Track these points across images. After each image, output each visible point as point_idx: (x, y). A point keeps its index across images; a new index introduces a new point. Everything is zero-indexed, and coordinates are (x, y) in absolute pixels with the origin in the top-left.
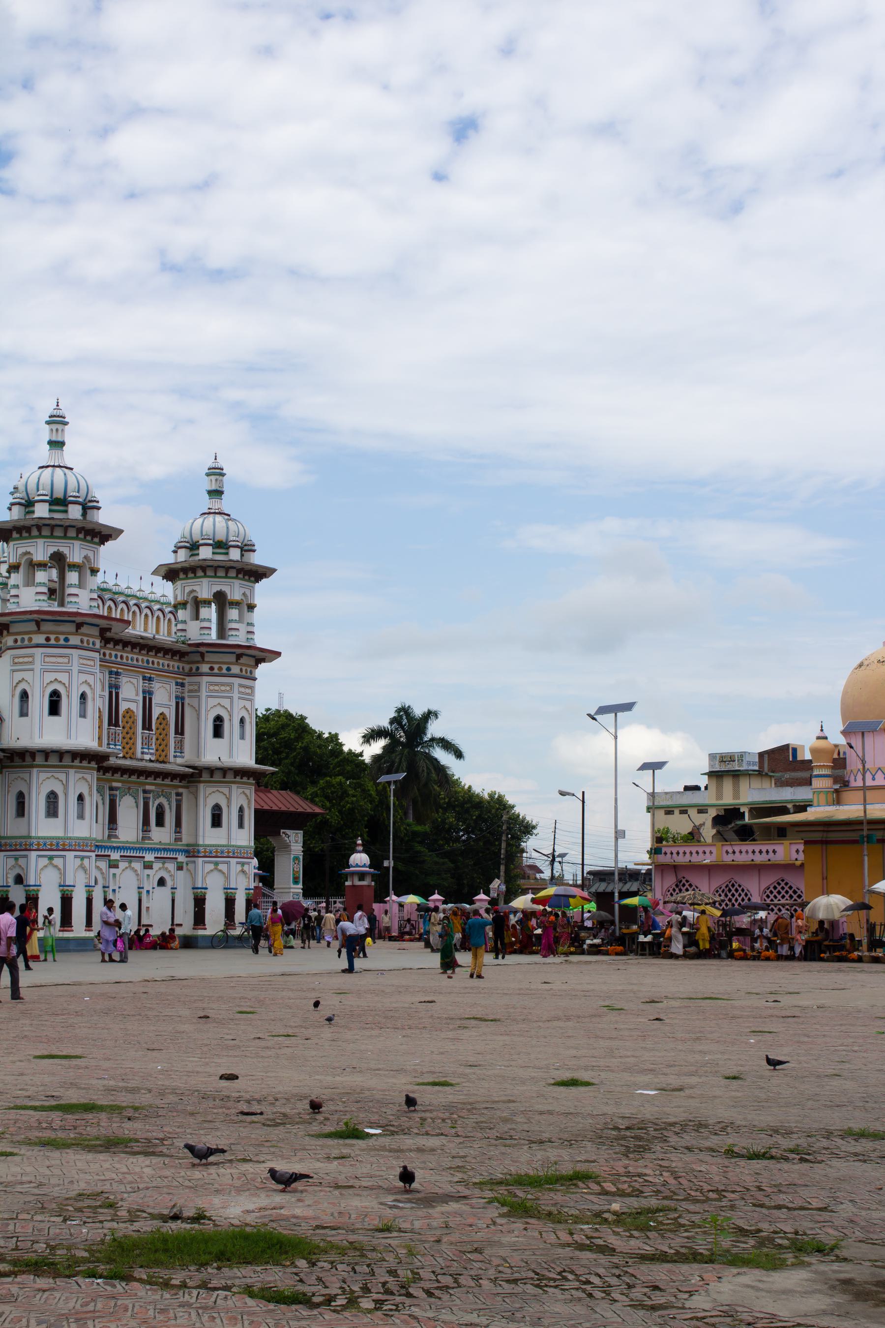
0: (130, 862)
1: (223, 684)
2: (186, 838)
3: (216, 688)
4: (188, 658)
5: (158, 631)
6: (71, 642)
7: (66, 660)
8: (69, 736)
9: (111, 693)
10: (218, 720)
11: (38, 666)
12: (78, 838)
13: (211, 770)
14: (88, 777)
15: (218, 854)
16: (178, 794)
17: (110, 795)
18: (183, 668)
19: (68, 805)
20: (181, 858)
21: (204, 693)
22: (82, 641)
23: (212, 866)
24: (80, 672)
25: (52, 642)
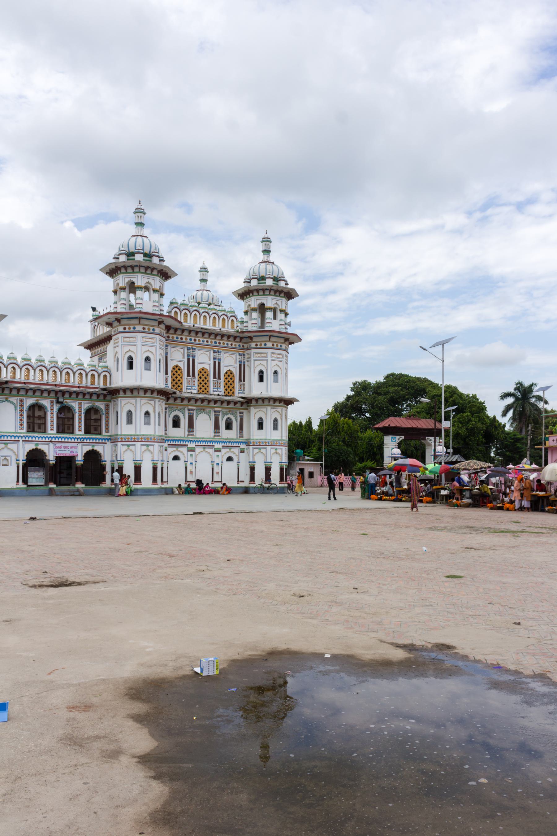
0: (204, 448)
1: (262, 353)
2: (245, 437)
3: (259, 355)
4: (243, 340)
5: (224, 326)
6: (136, 330)
7: (134, 339)
8: (136, 381)
9: (189, 360)
10: (261, 372)
11: (120, 344)
12: (143, 435)
13: (257, 400)
14: (152, 402)
15: (261, 444)
16: (240, 413)
17: (189, 413)
18: (243, 346)
19: (139, 417)
20: (243, 446)
21: (252, 359)
22: (144, 329)
23: (257, 451)
24: (143, 345)
25: (127, 330)
